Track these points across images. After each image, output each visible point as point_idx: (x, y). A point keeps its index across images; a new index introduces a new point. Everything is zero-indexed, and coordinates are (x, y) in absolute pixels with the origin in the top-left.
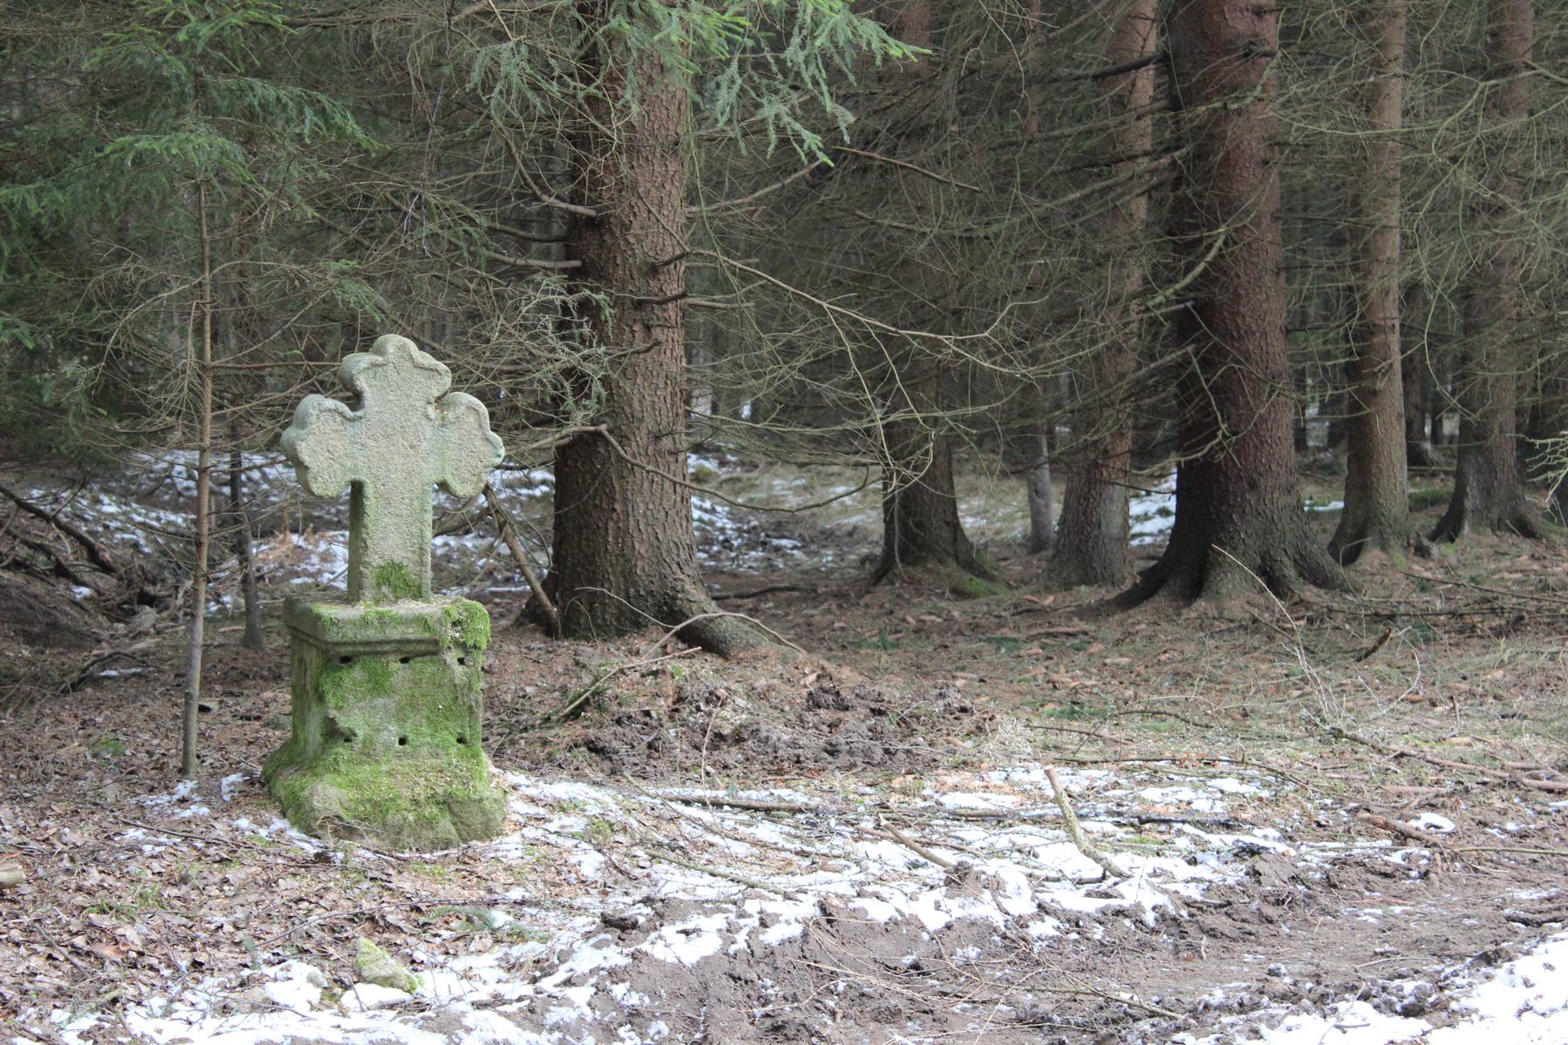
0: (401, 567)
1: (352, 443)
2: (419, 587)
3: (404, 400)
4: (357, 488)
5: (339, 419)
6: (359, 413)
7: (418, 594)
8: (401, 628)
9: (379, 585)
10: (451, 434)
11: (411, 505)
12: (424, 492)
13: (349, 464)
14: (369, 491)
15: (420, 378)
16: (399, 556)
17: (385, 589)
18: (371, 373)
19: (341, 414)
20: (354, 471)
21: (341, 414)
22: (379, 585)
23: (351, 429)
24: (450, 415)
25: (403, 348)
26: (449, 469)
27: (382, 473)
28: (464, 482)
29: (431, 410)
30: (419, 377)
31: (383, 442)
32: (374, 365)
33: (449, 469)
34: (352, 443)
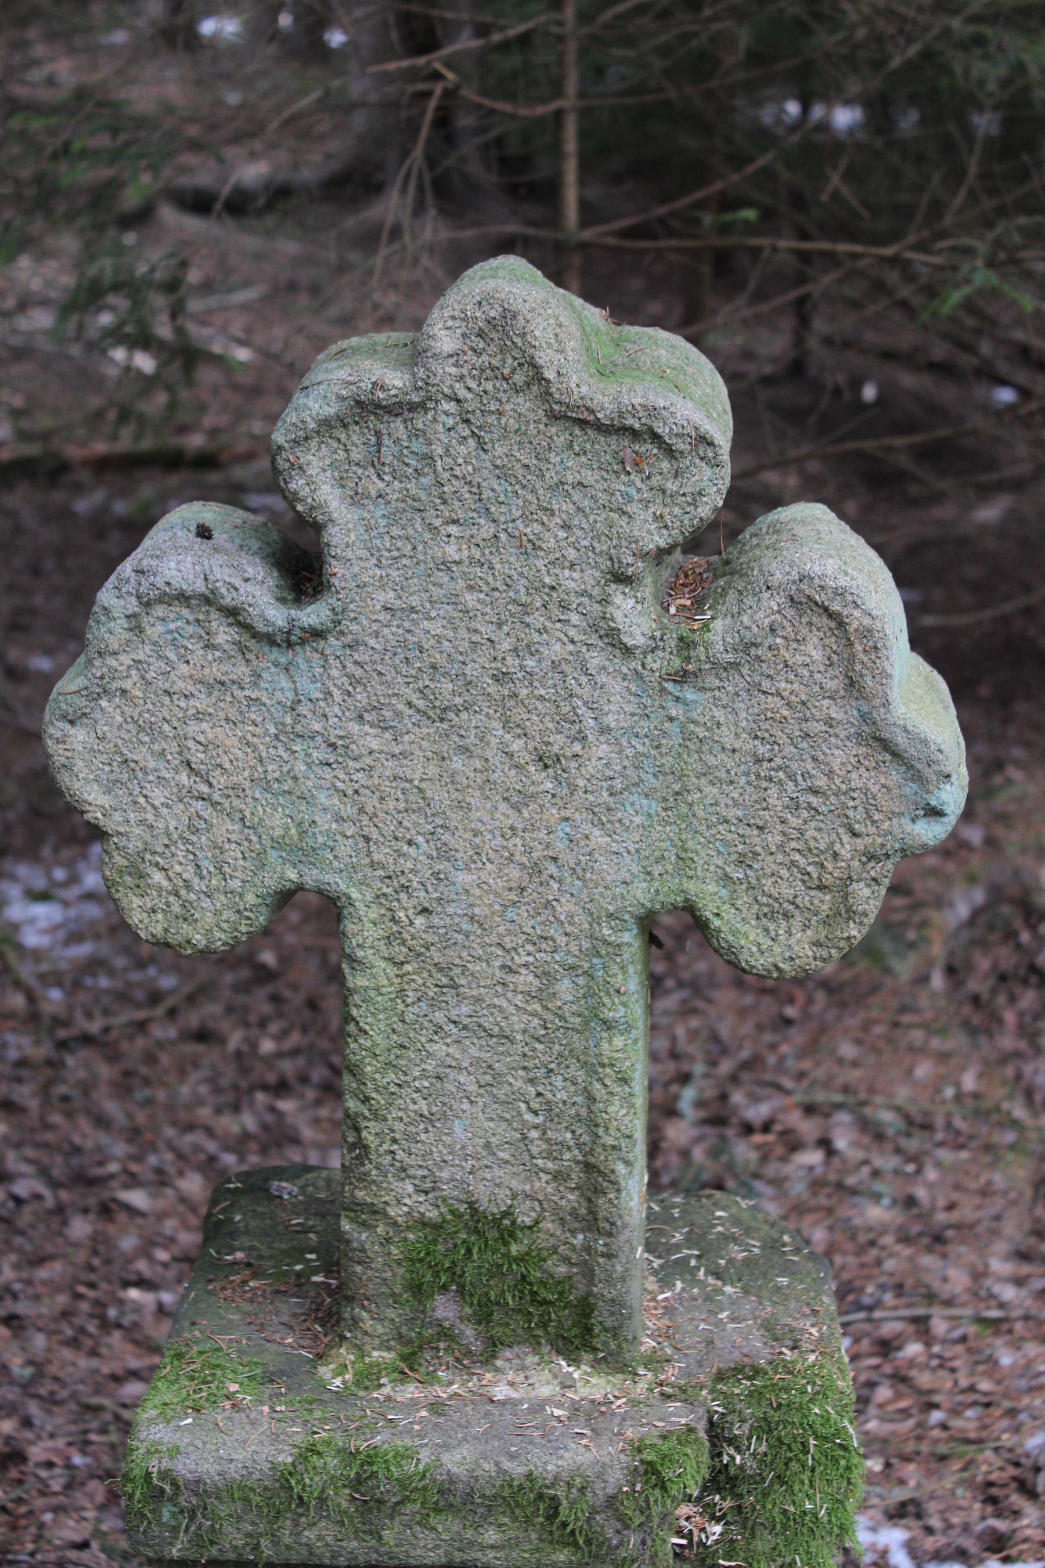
0: (503, 1228)
1: (285, 736)
2: (585, 1308)
3: (508, 562)
4: (311, 917)
5: (224, 634)
6: (314, 614)
7: (578, 1324)
8: (448, 1526)
9: (417, 1290)
10: (723, 714)
11: (543, 995)
12: (601, 949)
13: (277, 822)
14: (364, 930)
15: (576, 469)
16: (498, 1186)
17: (444, 1308)
18: (358, 441)
19: (233, 614)
20: (300, 850)
21: (233, 614)
22: (417, 1290)
23: (275, 682)
24: (719, 632)
25: (500, 329)
26: (708, 859)
27: (417, 858)
28: (774, 912)
29: (634, 614)
30: (574, 464)
31: (420, 737)
32: (368, 408)
33: (708, 859)
34: (285, 736)
